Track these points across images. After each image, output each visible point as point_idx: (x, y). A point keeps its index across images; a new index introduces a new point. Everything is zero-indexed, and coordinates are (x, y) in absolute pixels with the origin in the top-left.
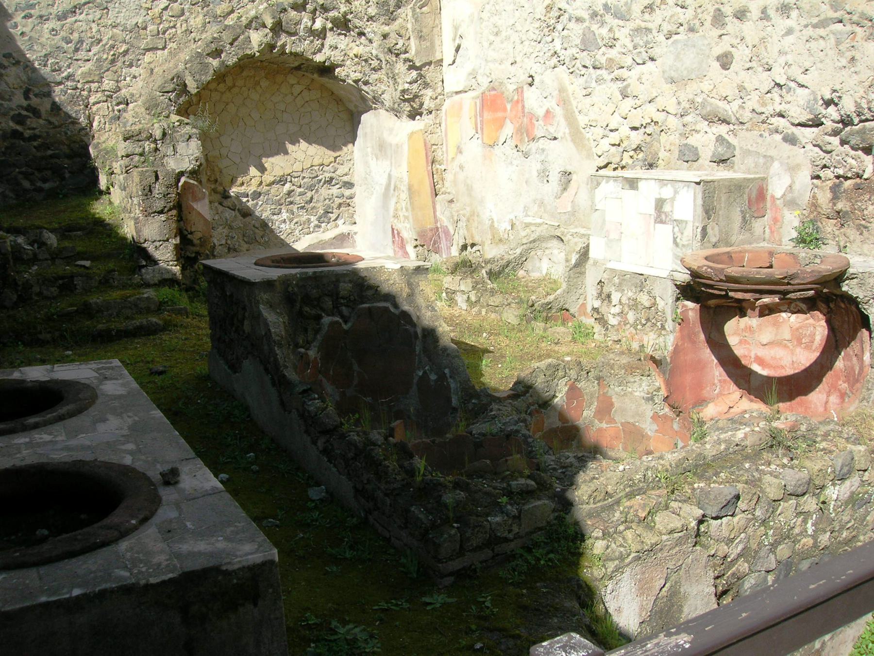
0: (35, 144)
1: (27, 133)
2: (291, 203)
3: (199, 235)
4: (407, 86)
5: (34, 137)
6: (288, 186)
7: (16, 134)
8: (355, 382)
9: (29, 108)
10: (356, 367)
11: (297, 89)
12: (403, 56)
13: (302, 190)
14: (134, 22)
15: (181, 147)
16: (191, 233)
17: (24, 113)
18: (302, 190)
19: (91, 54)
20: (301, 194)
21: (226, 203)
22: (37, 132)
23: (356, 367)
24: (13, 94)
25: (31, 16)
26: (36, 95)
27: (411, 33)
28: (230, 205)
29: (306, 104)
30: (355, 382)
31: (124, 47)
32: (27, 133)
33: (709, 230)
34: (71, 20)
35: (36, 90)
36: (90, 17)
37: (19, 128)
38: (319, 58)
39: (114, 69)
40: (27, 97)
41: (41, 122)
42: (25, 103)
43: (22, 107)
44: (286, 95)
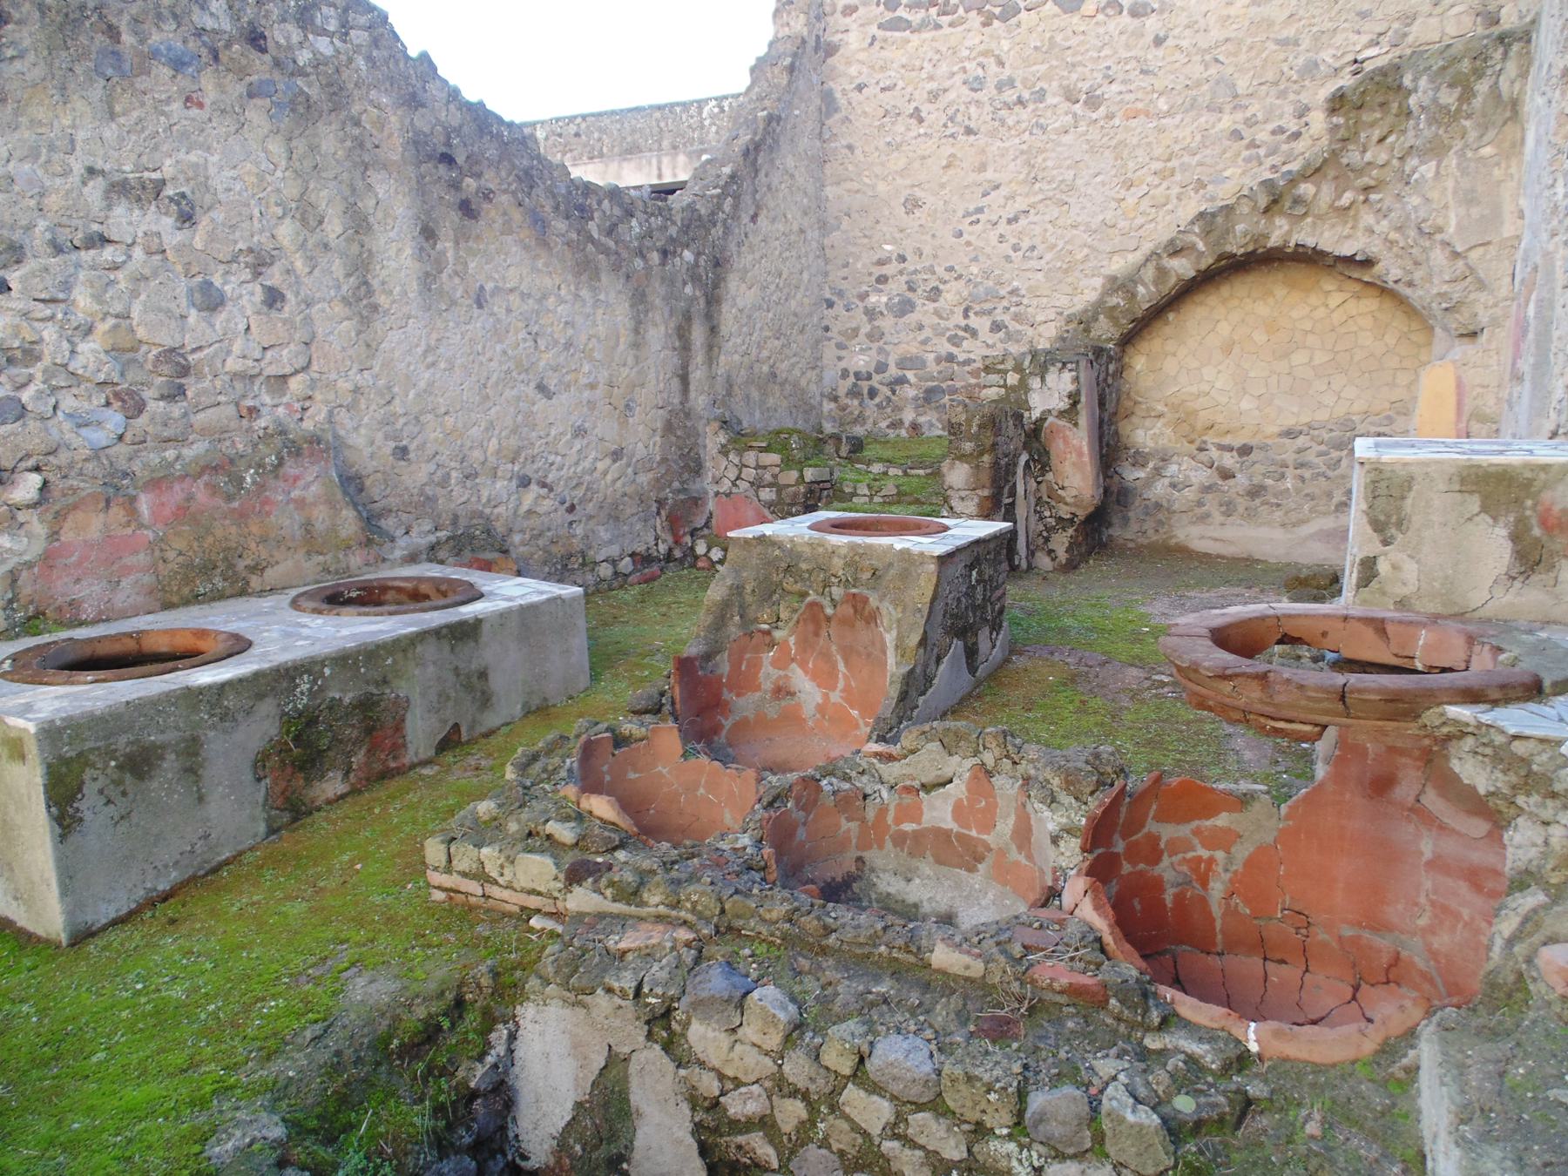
0: (967, 368)
1: (961, 357)
2: (1302, 465)
3: (1074, 492)
4: (1445, 288)
5: (967, 362)
6: (1301, 441)
7: (951, 358)
8: (841, 685)
9: (966, 329)
10: (841, 666)
11: (1334, 300)
12: (1438, 237)
13: (1323, 448)
14: (1101, 217)
15: (1051, 377)
16: (1063, 488)
17: (961, 333)
18: (1323, 448)
19: (1043, 262)
20: (1320, 454)
21: (1202, 456)
22: (972, 356)
23: (841, 666)
24: (953, 312)
25: (978, 221)
26: (976, 314)
27: (1450, 197)
28: (1205, 459)
29: (1350, 322)
30: (841, 685)
31: (1086, 251)
32: (961, 357)
33: (1383, 567)
34: (1023, 222)
35: (977, 308)
36: (1047, 218)
37: (954, 350)
38: (1346, 250)
39: (1070, 280)
40: (966, 316)
41: (978, 343)
42: (963, 323)
43: (958, 326)
44: (1316, 308)
